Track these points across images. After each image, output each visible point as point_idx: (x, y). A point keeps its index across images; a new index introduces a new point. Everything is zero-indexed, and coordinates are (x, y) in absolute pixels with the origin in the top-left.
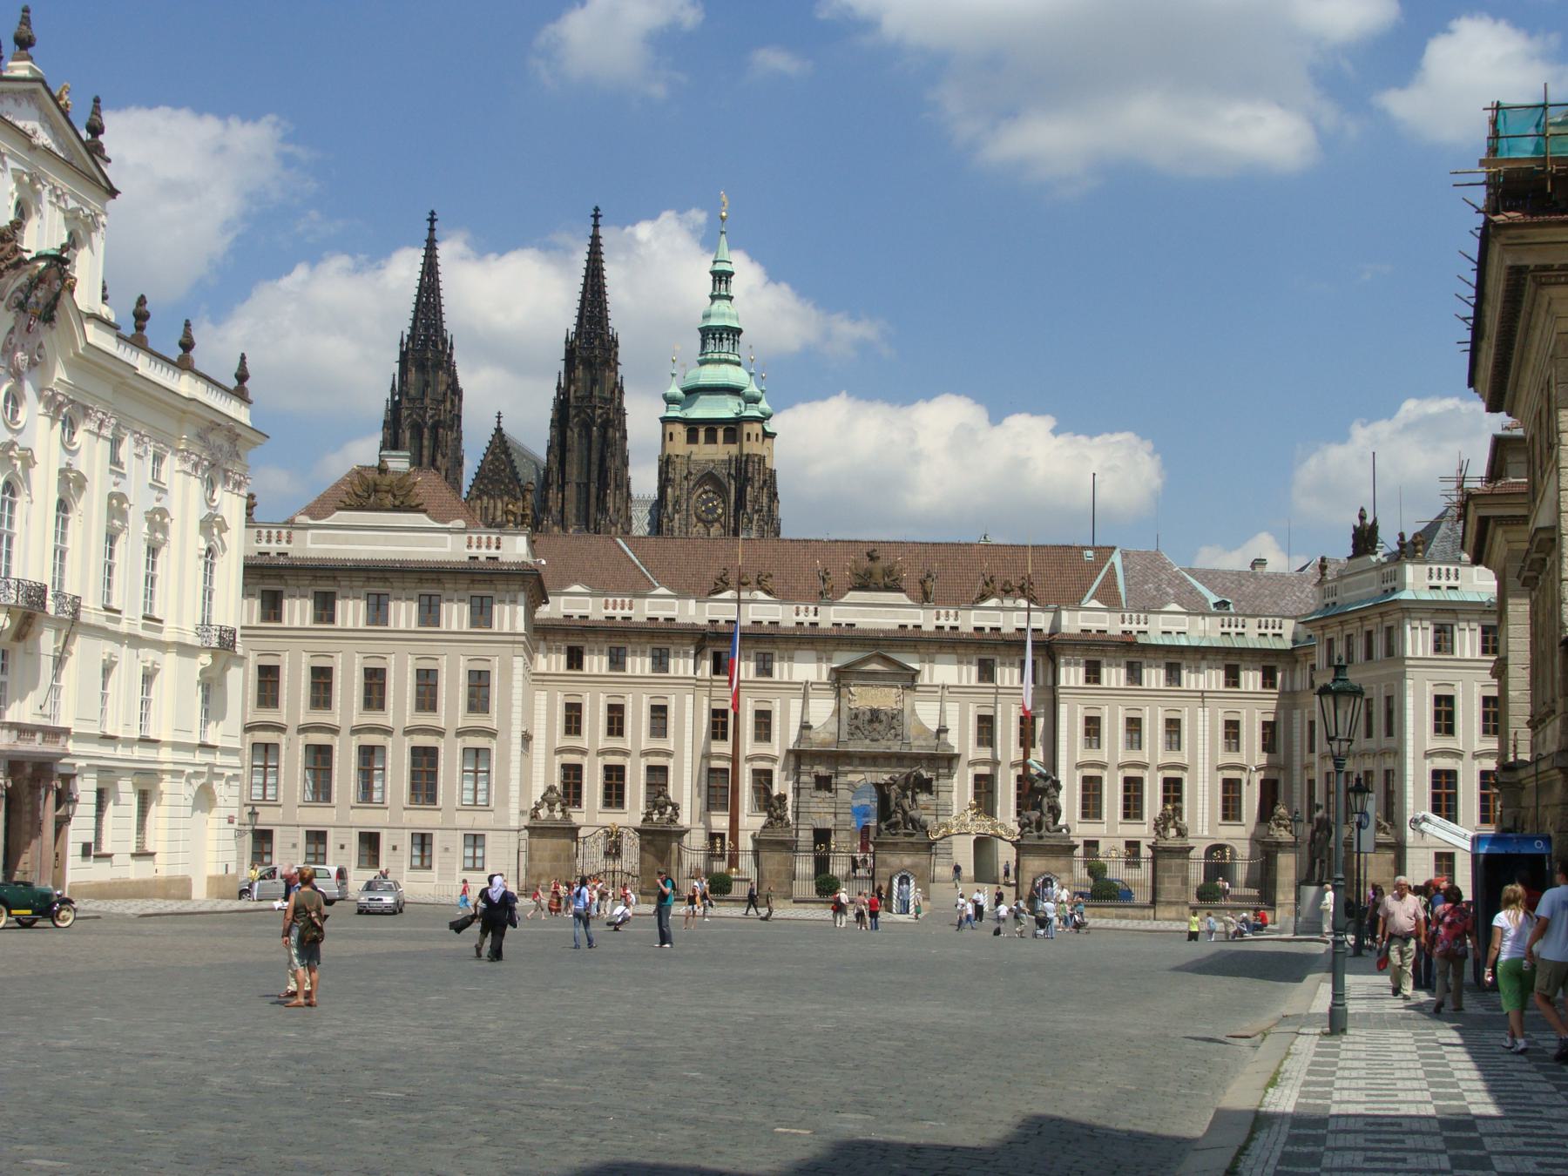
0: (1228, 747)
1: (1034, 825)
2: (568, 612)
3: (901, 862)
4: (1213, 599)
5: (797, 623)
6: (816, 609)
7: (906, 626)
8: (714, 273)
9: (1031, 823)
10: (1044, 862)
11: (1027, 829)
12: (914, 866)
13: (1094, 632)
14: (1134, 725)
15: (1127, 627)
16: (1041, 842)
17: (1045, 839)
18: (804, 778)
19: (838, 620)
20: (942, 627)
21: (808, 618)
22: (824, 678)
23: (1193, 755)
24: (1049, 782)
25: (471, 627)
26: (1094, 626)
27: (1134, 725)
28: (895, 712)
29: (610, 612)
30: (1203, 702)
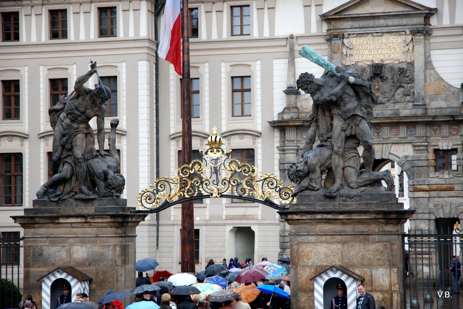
3: (69, 253)
11: (305, 183)
22: (314, 30)
28: (404, 66)
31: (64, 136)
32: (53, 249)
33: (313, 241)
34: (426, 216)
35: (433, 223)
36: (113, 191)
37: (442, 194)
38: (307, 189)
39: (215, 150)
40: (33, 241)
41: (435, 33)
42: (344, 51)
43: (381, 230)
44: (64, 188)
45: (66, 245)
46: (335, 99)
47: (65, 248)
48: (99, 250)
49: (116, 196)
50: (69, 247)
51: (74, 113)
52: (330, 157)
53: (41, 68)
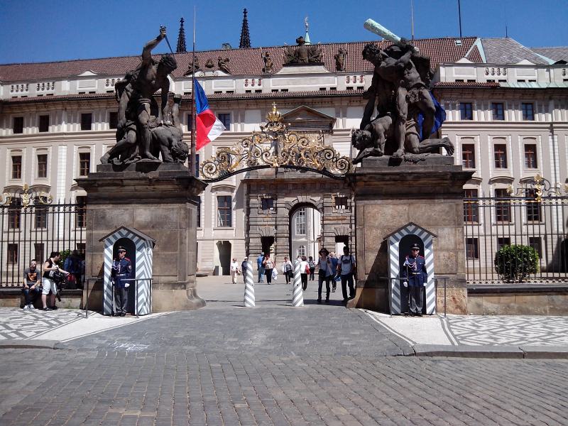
2: (82, 90)
3: (133, 218)
5: (247, 91)
7: (325, 89)
12: (154, 225)
13: (465, 81)
14: (500, 151)
15: (490, 77)
16: (396, 170)
17: (403, 165)
18: (253, 201)
19: (275, 88)
20: (352, 88)
21: (253, 89)
23: (547, 170)
25: (82, 129)
27: (500, 151)
30: (552, 132)
34: (331, 234)
35: (334, 238)
41: (335, 133)
46: (403, 66)
47: (128, 211)
48: (164, 214)
53: (104, 146)
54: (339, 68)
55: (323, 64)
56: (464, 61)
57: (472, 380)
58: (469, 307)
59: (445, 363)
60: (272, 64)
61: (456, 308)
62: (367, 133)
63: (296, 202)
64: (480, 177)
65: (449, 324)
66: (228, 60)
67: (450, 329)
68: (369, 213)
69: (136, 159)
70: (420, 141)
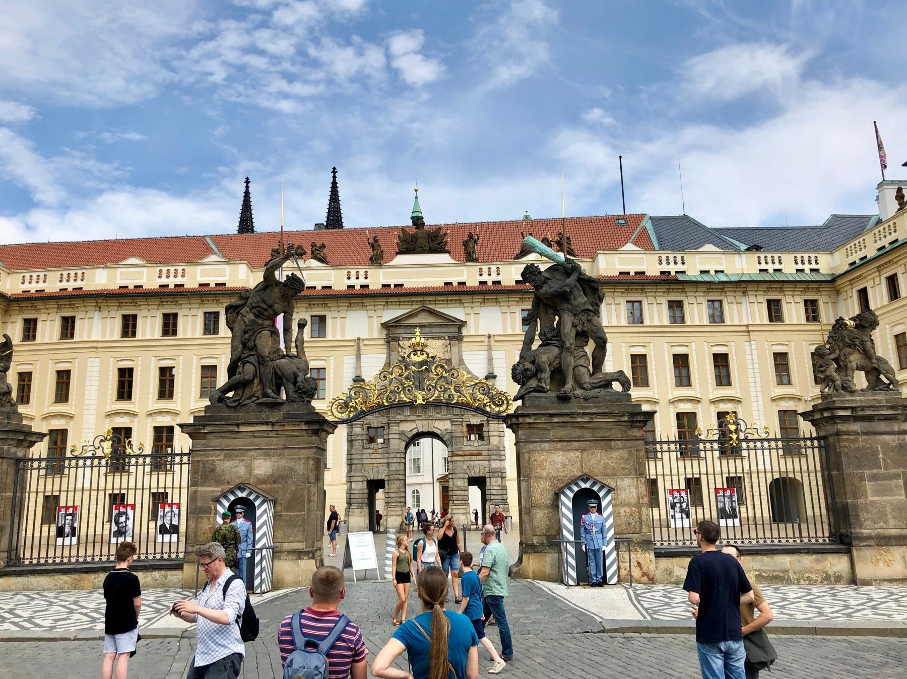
0: (780, 383)
1: (546, 375)
2: (124, 283)
4: (743, 247)
5: (349, 287)
6: (366, 272)
7: (451, 284)
8: (412, 218)
9: (539, 370)
10: (574, 455)
11: (533, 383)
12: (274, 479)
13: (632, 273)
14: (681, 362)
15: (665, 267)
19: (386, 282)
20: (485, 283)
21: (358, 284)
24: (572, 280)
26: (632, 269)
27: (681, 362)
29: (164, 281)
31: (245, 332)
32: (228, 464)
33: (546, 448)
34: (462, 475)
35: (466, 480)
36: (303, 396)
37: (473, 458)
38: (535, 390)
39: (419, 353)
40: (202, 455)
41: (465, 339)
42: (400, 350)
43: (625, 435)
44: (243, 393)
45: (246, 458)
46: (568, 290)
47: (244, 463)
49: (308, 401)
50: (249, 462)
51: (259, 307)
52: (559, 357)
54: (470, 257)
55: (449, 252)
56: (630, 247)
57: (671, 657)
58: (659, 575)
59: (638, 640)
60: (382, 252)
61: (643, 576)
62: (528, 366)
63: (415, 432)
64: (656, 397)
65: (637, 596)
66: (323, 246)
67: (639, 601)
68: (535, 460)
69: (254, 399)
70: (591, 375)
